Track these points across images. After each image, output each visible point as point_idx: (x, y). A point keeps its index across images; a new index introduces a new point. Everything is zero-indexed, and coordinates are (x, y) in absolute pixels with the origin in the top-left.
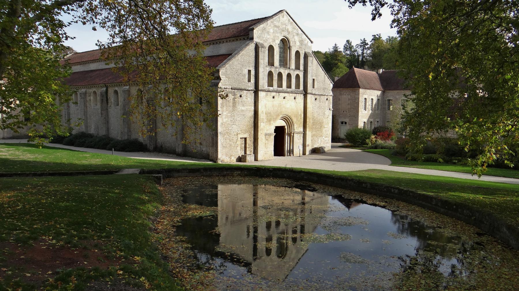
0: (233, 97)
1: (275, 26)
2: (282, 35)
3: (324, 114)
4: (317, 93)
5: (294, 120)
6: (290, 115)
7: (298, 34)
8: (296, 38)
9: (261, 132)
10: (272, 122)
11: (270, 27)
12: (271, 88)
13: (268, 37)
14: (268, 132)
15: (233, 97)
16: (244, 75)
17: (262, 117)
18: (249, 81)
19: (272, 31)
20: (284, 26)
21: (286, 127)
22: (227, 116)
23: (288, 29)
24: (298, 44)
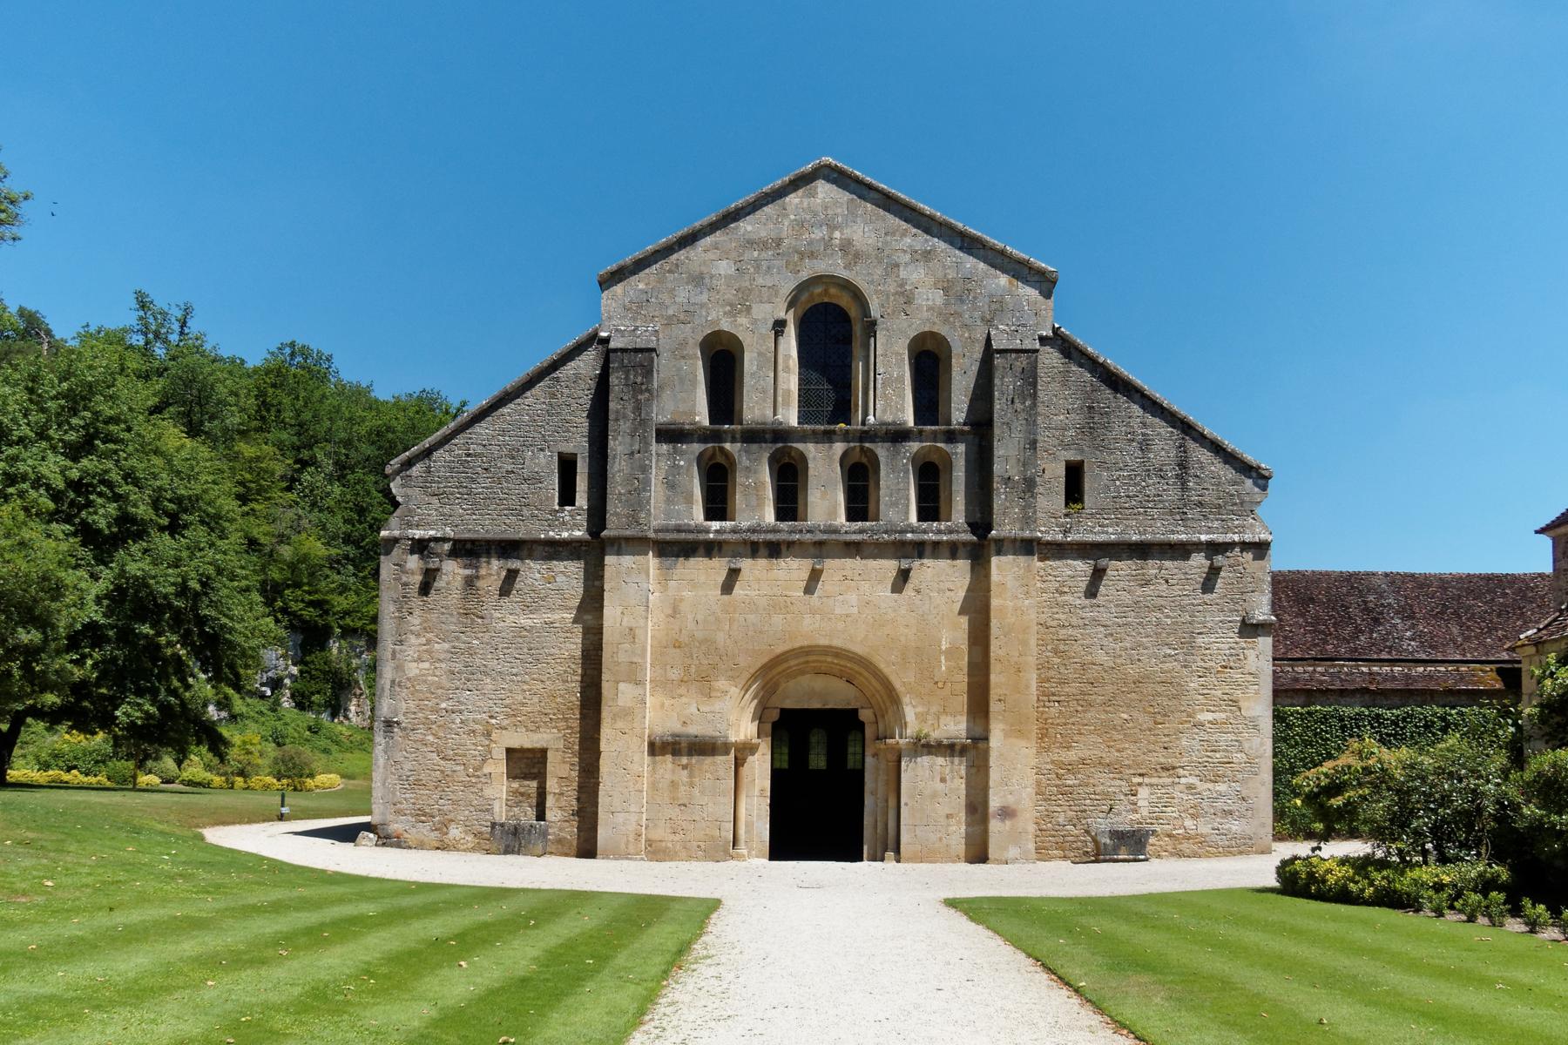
0: (468, 572)
1: (751, 243)
2: (805, 275)
3: (1189, 646)
4: (1111, 535)
5: (900, 680)
6: (859, 649)
7: (927, 255)
8: (916, 275)
9: (620, 724)
10: (722, 684)
11: (710, 255)
12: (715, 525)
13: (704, 298)
14: (693, 730)
15: (468, 572)
16: (534, 479)
17: (622, 658)
18: (567, 497)
19: (725, 268)
20: (818, 234)
21: (865, 715)
22: (427, 655)
23: (846, 246)
24: (929, 297)
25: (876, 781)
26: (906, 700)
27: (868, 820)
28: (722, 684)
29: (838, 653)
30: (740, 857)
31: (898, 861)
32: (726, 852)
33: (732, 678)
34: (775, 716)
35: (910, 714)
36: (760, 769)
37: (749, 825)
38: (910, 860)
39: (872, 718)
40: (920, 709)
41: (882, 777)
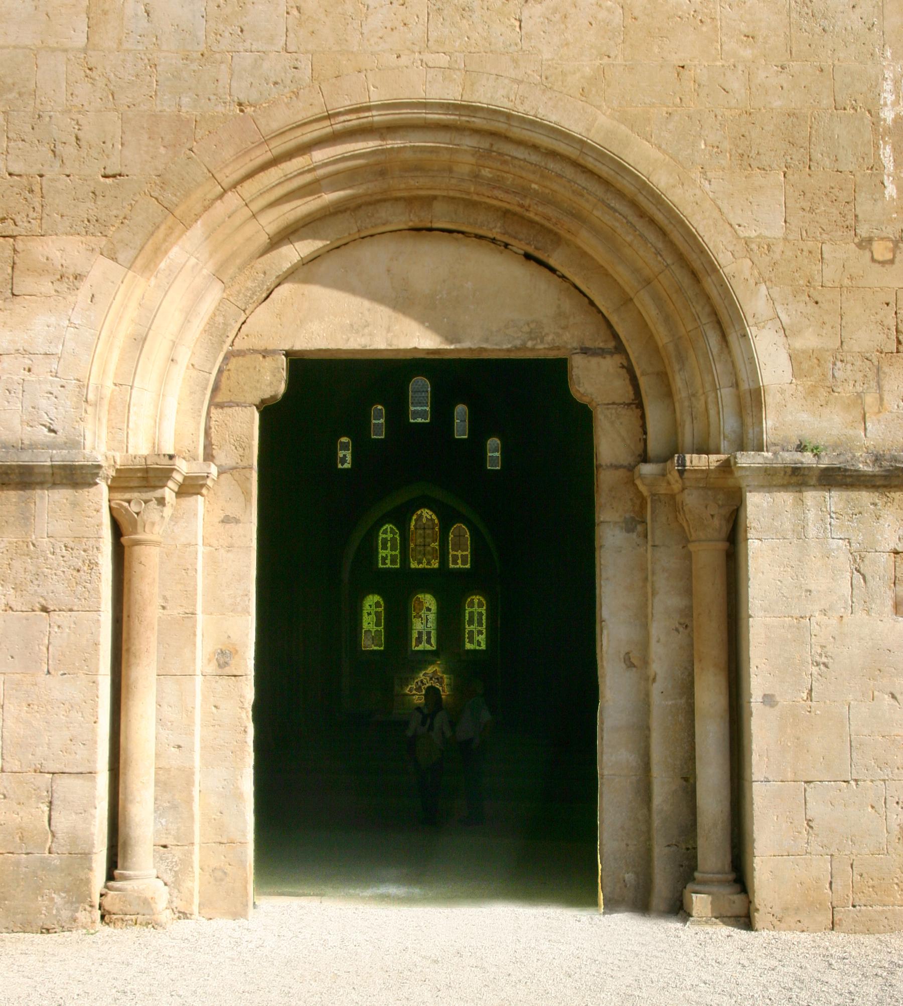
5: (738, 221)
25: (642, 618)
26: (755, 303)
27: (613, 756)
28: (61, 249)
29: (493, 132)
30: (141, 916)
31: (746, 921)
32: (77, 893)
33: (95, 225)
34: (273, 382)
35: (771, 359)
36: (211, 567)
37: (173, 787)
38: (778, 923)
39: (620, 388)
40: (809, 340)
41: (666, 601)
